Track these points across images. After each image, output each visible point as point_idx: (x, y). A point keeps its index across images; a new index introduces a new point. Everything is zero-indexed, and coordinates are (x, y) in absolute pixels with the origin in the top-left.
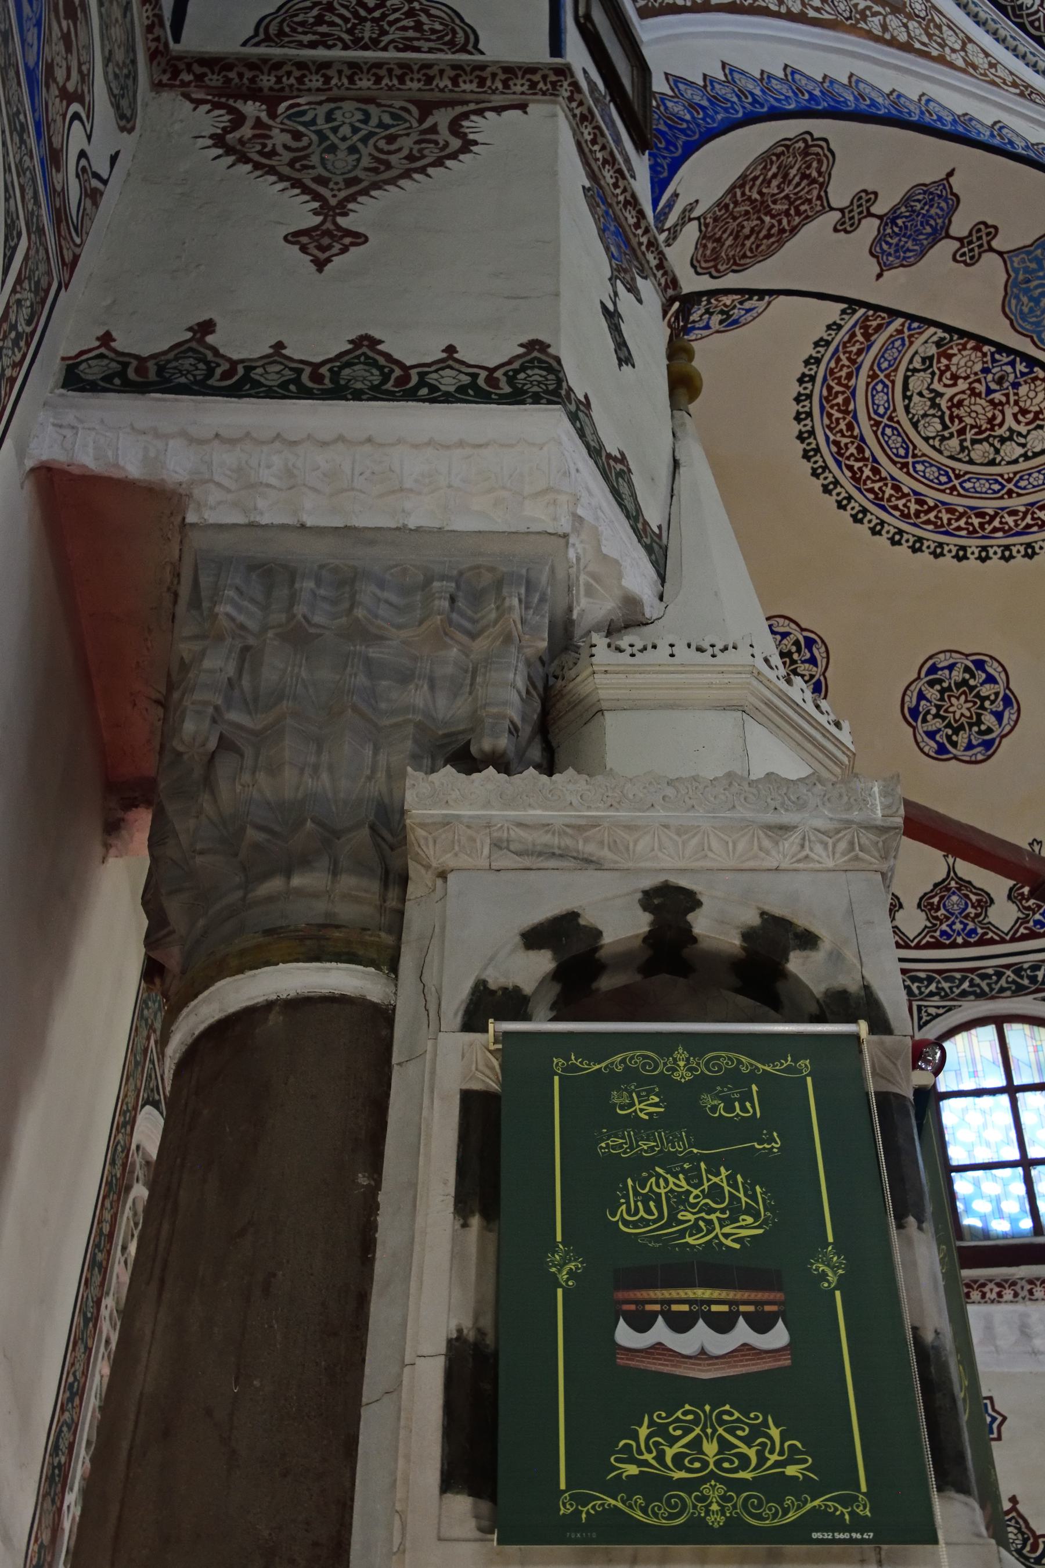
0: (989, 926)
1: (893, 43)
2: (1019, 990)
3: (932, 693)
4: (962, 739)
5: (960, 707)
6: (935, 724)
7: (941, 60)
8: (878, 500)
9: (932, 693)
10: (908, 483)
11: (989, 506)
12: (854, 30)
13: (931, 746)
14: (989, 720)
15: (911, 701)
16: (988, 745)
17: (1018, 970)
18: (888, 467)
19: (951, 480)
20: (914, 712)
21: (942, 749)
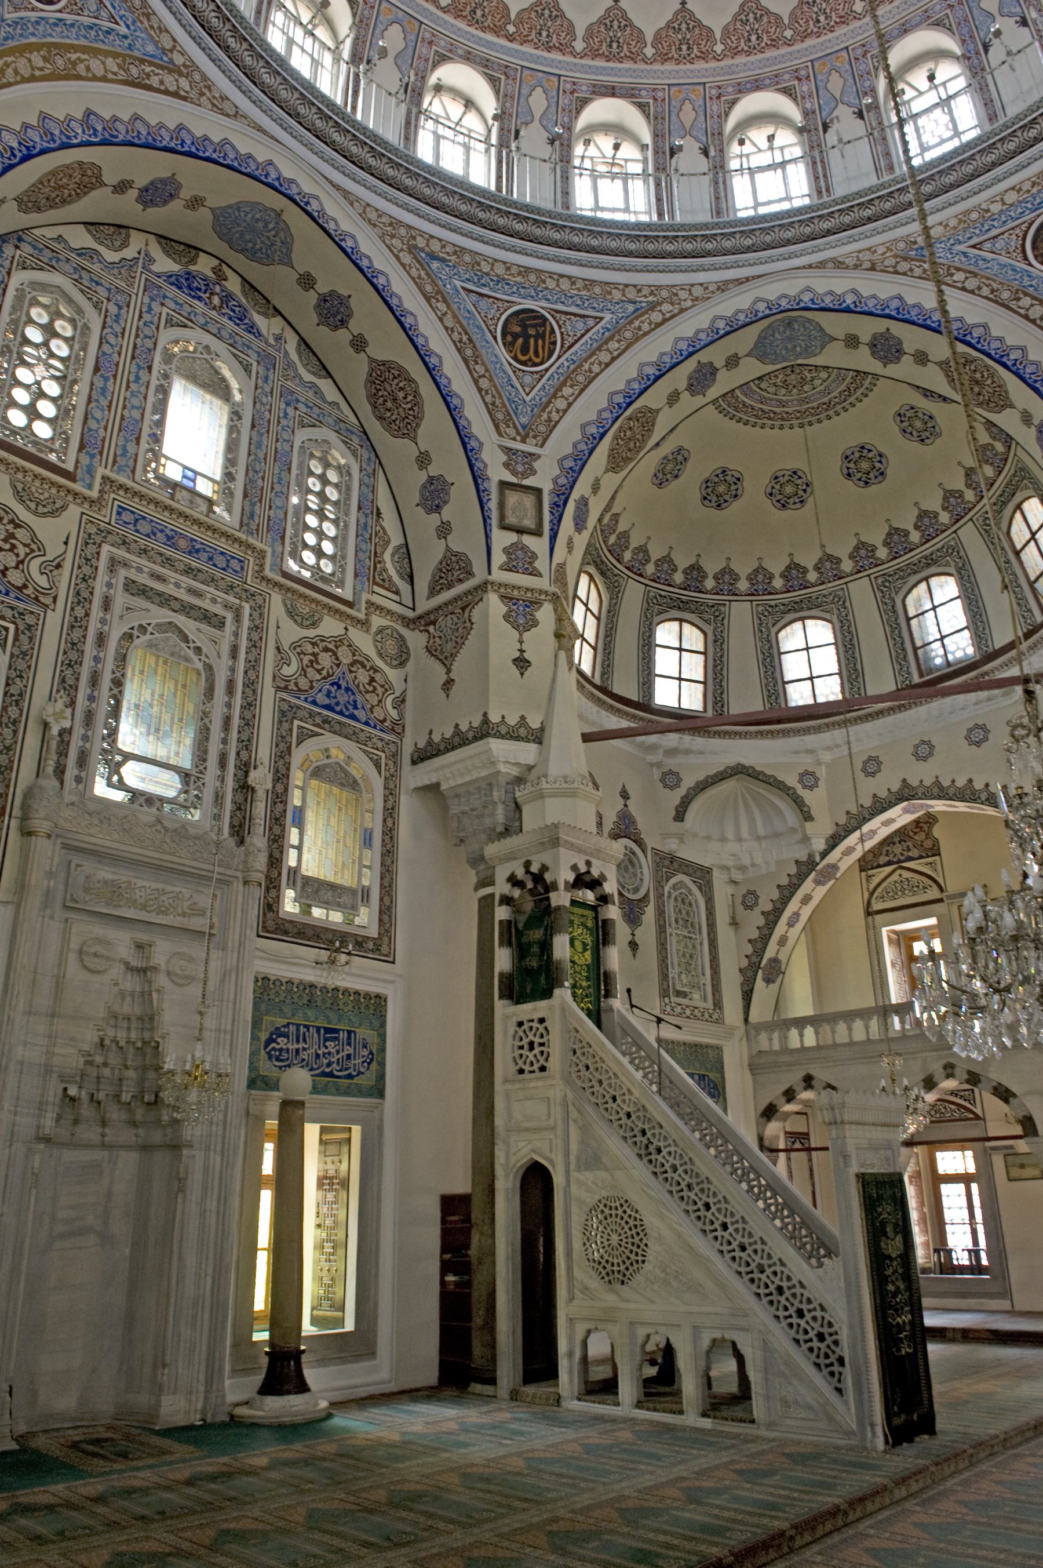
0: (911, 543)
1: (658, 325)
2: (928, 565)
3: (852, 465)
4: (872, 476)
5: (865, 465)
6: (859, 475)
7: (682, 311)
8: (783, 419)
9: (852, 465)
10: (790, 410)
11: (826, 400)
12: (637, 339)
13: (862, 484)
14: (878, 465)
15: (845, 471)
16: (882, 474)
17: (926, 557)
18: (777, 410)
19: (802, 401)
20: (849, 475)
21: (866, 483)
